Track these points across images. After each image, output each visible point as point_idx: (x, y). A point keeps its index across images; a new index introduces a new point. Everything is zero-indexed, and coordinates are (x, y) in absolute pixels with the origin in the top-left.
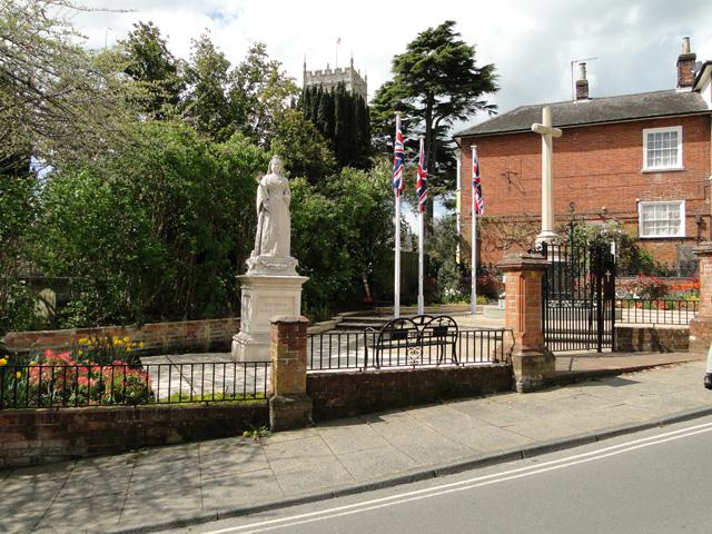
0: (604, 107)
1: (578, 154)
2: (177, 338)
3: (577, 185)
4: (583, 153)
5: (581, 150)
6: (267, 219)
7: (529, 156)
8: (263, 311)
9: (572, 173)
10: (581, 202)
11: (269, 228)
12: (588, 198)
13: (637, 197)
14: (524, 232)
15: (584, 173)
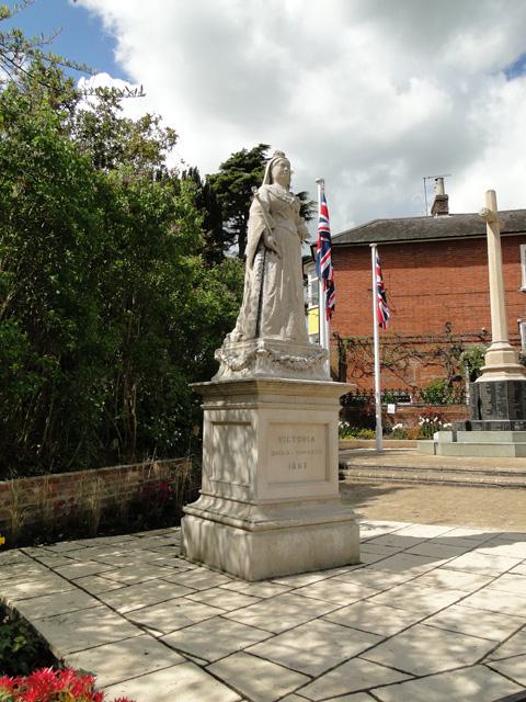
0: (471, 222)
1: (453, 269)
2: (33, 508)
3: (453, 303)
4: (458, 269)
5: (456, 266)
6: (272, 268)
7: (400, 271)
8: (274, 454)
9: (447, 289)
10: (458, 322)
11: (277, 284)
12: (465, 319)
13: (519, 317)
14: (396, 356)
15: (460, 289)
